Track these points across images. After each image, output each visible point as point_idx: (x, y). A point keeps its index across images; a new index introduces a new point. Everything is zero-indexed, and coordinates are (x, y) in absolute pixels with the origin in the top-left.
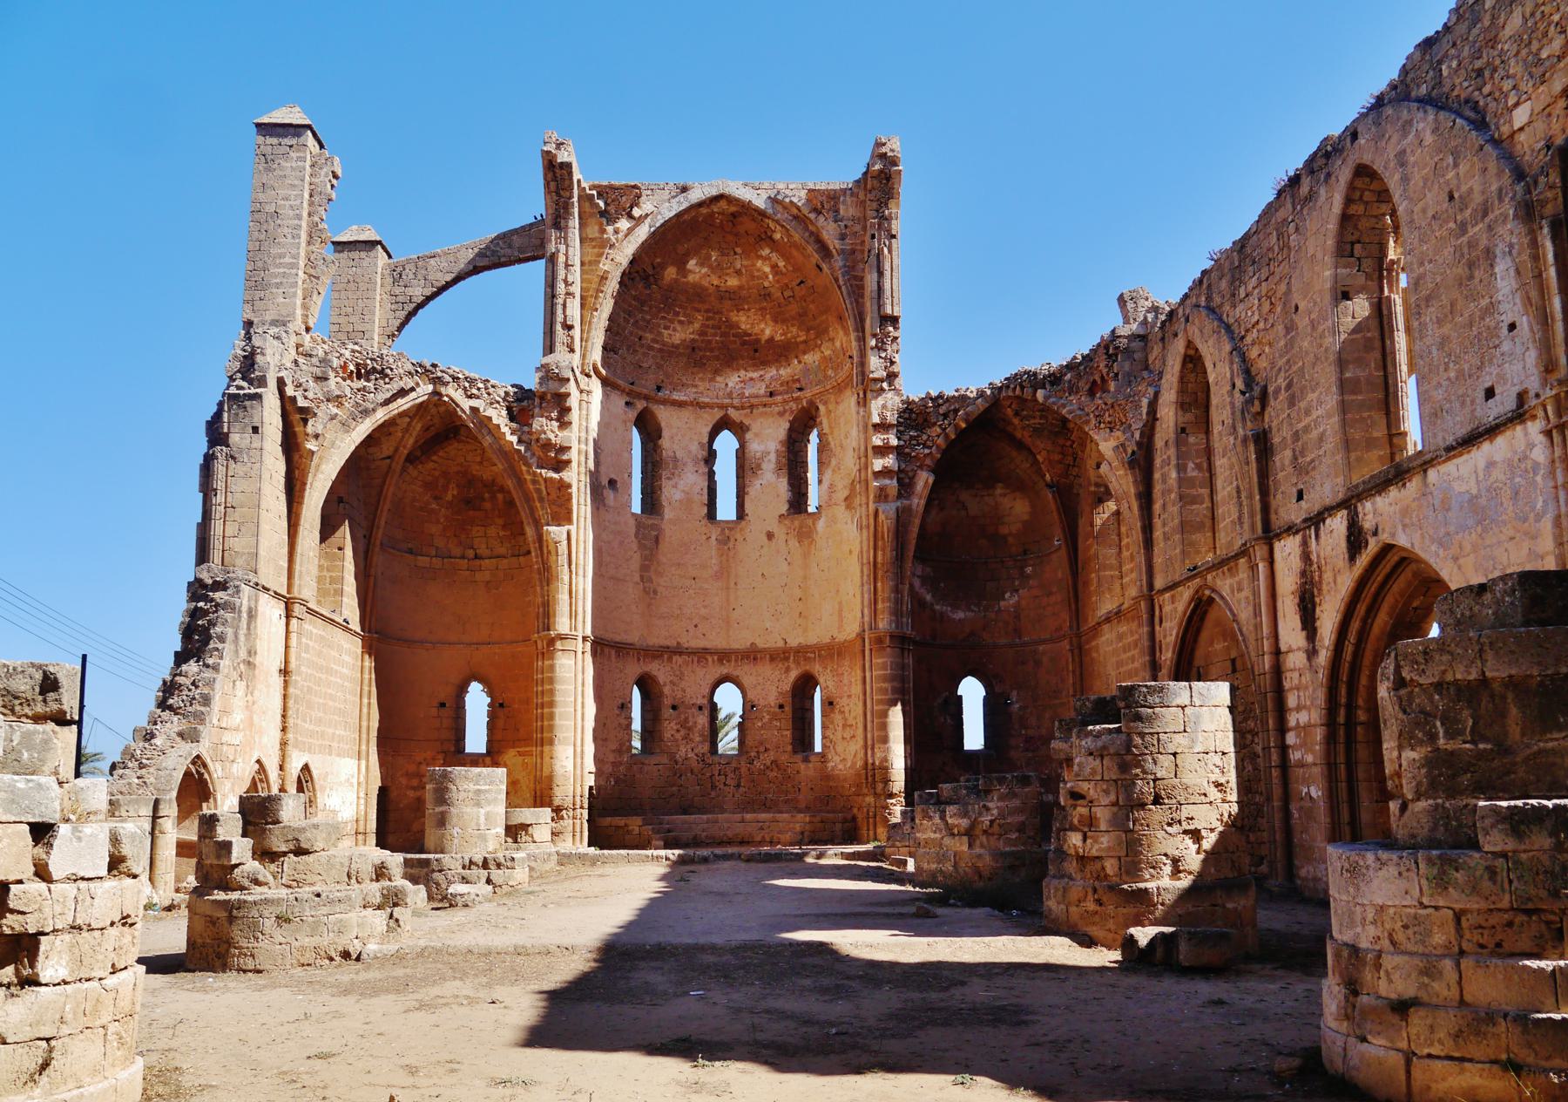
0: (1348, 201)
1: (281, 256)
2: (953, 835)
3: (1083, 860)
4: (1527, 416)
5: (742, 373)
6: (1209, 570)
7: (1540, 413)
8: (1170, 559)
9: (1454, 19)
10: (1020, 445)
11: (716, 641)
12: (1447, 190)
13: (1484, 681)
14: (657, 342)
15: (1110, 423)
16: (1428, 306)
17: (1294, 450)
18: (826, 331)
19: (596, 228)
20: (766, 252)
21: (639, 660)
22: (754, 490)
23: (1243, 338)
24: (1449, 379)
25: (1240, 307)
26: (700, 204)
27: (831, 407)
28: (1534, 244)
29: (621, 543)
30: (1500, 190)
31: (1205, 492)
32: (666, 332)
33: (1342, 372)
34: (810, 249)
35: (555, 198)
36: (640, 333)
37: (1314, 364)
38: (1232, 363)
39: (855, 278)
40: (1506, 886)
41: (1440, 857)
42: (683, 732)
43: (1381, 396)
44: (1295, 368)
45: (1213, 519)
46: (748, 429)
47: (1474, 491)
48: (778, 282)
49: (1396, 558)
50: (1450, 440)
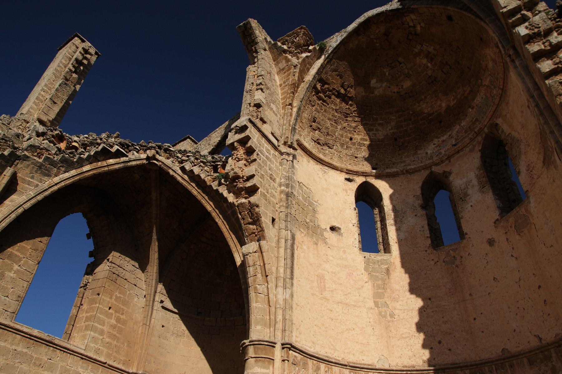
5: (436, 141)
29: (350, 275)
36: (349, 135)
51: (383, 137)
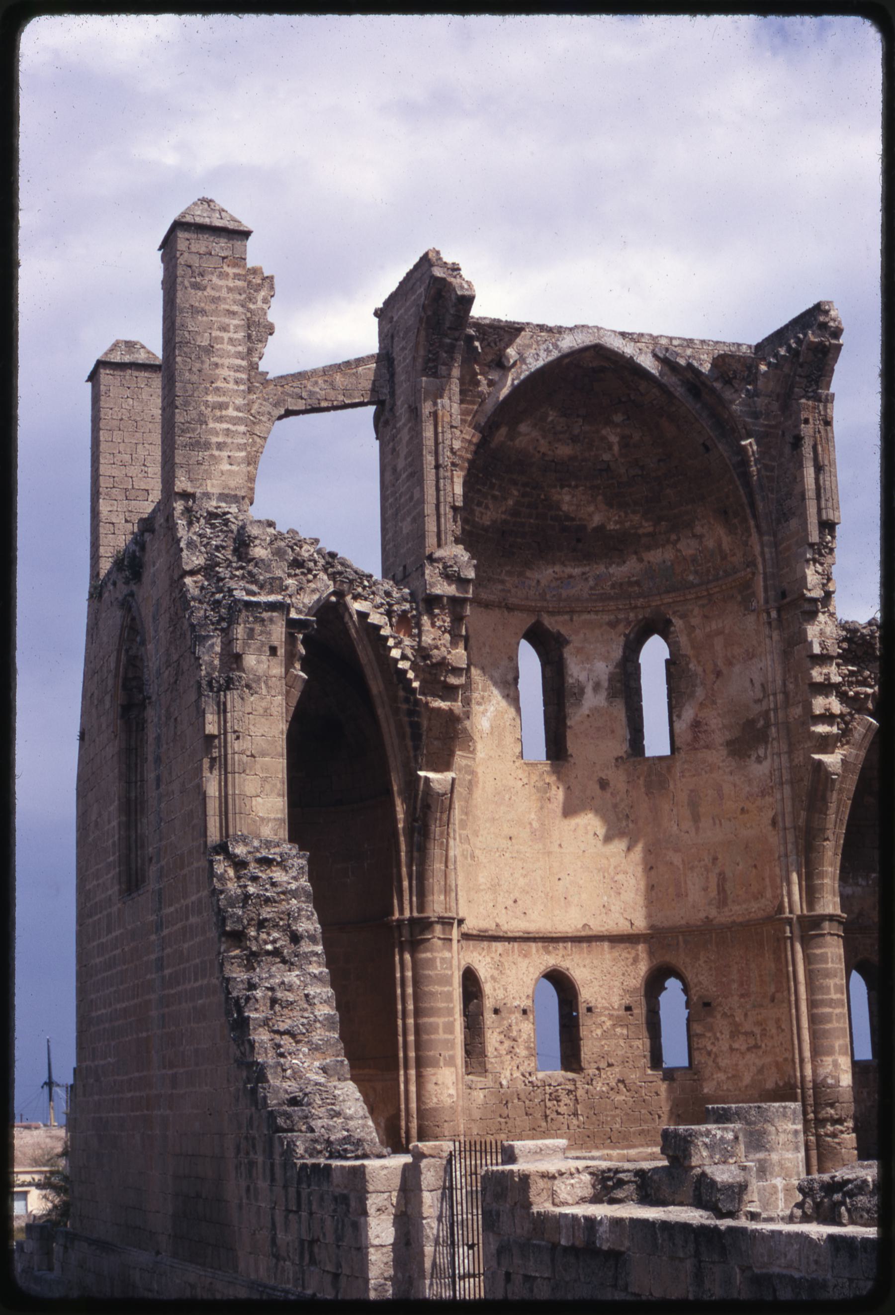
1: (222, 406)
5: (557, 568)
22: (576, 718)
42: (507, 1044)
46: (567, 642)
51: (488, 523)
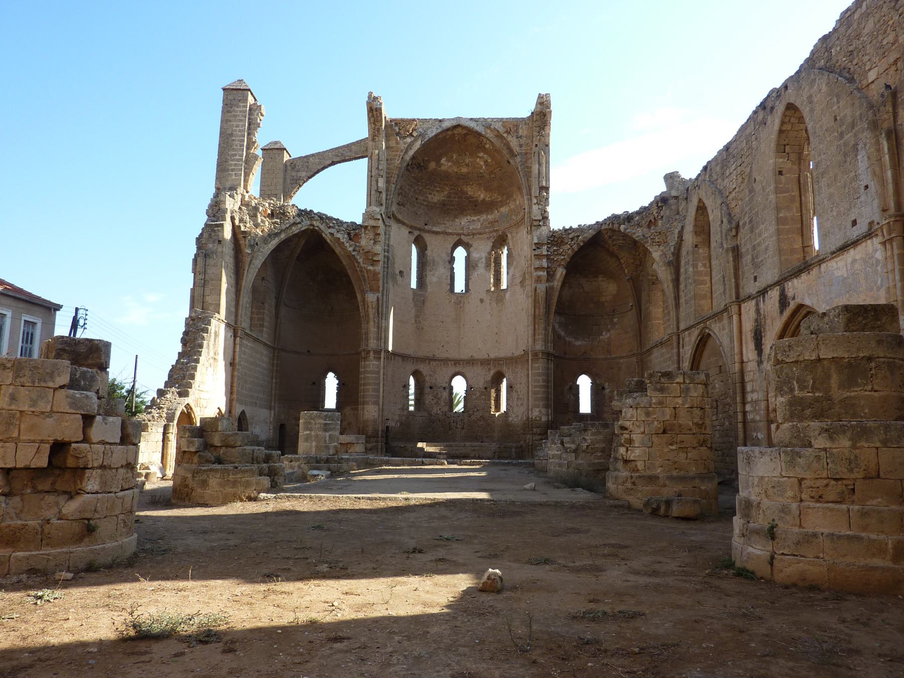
0: (783, 123)
1: (235, 155)
2: (567, 452)
3: (626, 462)
4: (873, 235)
5: (469, 217)
6: (708, 319)
7: (879, 233)
8: (688, 313)
9: (838, 25)
10: (612, 254)
11: (453, 354)
12: (833, 115)
13: (819, 360)
14: (424, 200)
15: (658, 242)
16: (822, 178)
17: (752, 256)
18: (512, 196)
19: (394, 141)
20: (481, 154)
21: (413, 363)
22: (475, 276)
23: (727, 197)
24: (833, 216)
25: (726, 181)
26: (448, 130)
27: (514, 235)
28: (878, 143)
30: (861, 115)
31: (708, 278)
32: (430, 196)
33: (778, 214)
34: (505, 152)
35: (373, 126)
36: (417, 196)
37: (764, 209)
38: (721, 210)
39: (527, 167)
40: (825, 466)
41: (791, 451)
42: (435, 400)
43: (799, 226)
44: (754, 212)
45: (712, 293)
46: (471, 246)
47: (845, 275)
48: (487, 170)
49: (804, 312)
50: (833, 248)
